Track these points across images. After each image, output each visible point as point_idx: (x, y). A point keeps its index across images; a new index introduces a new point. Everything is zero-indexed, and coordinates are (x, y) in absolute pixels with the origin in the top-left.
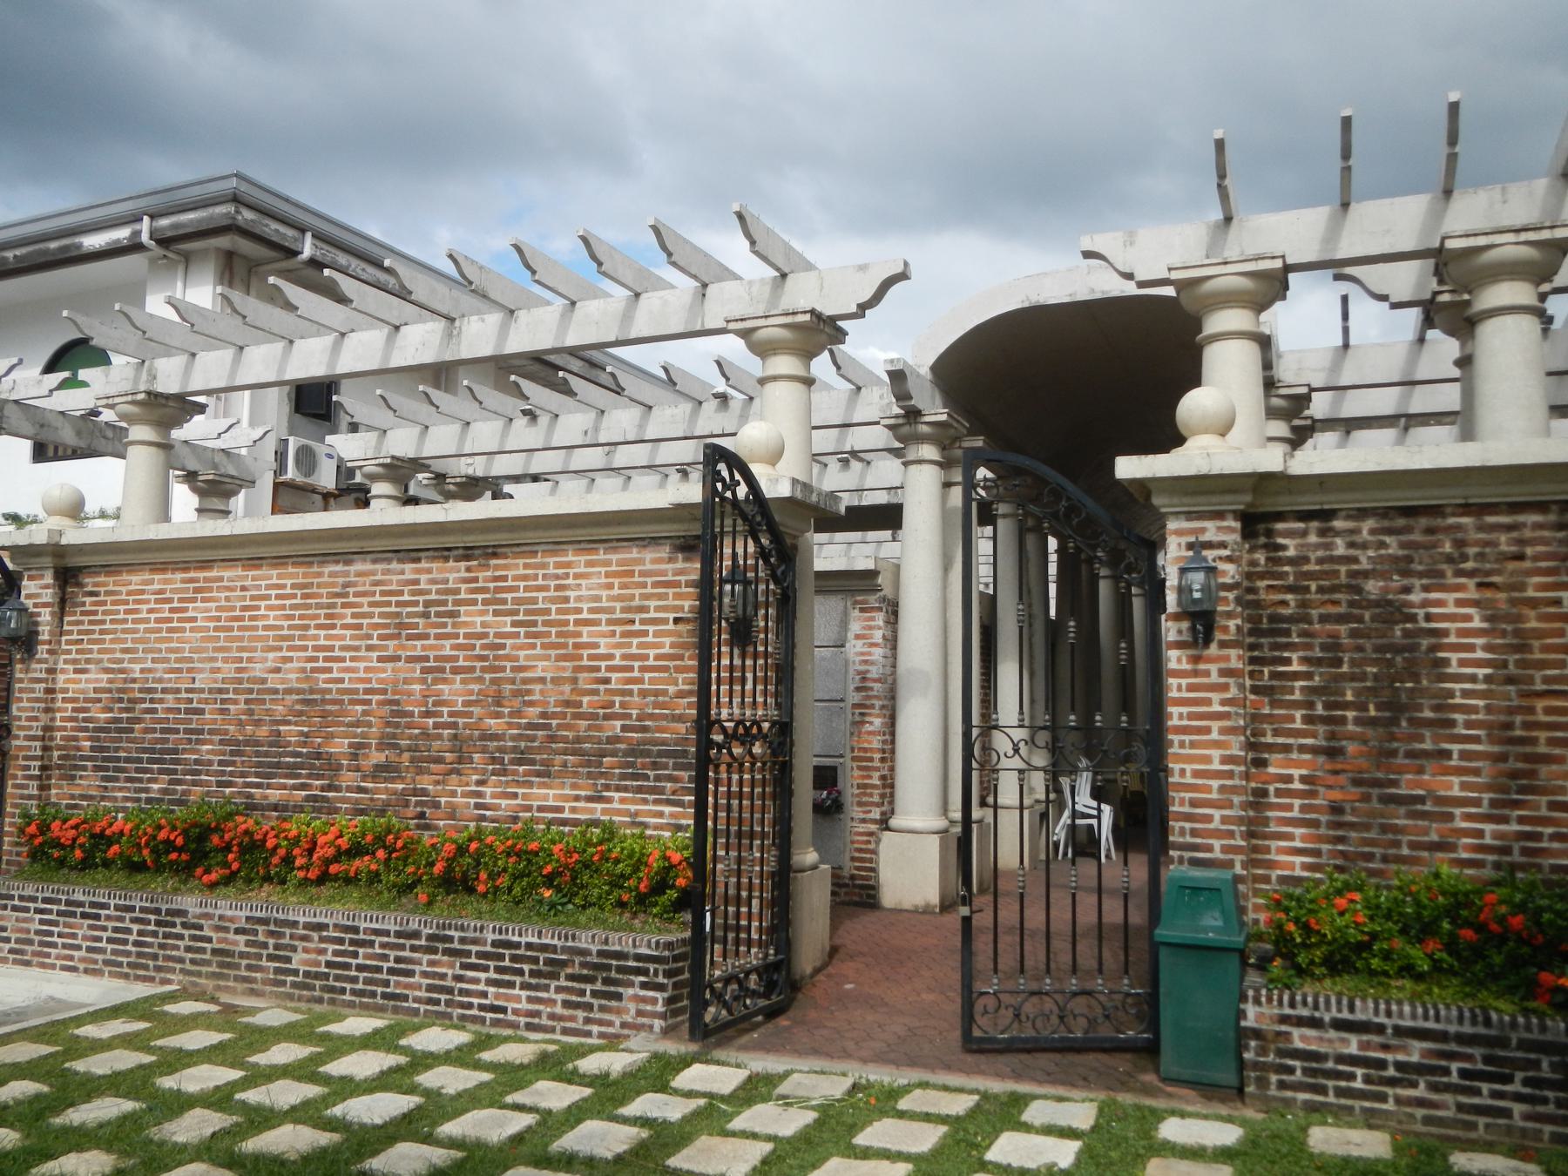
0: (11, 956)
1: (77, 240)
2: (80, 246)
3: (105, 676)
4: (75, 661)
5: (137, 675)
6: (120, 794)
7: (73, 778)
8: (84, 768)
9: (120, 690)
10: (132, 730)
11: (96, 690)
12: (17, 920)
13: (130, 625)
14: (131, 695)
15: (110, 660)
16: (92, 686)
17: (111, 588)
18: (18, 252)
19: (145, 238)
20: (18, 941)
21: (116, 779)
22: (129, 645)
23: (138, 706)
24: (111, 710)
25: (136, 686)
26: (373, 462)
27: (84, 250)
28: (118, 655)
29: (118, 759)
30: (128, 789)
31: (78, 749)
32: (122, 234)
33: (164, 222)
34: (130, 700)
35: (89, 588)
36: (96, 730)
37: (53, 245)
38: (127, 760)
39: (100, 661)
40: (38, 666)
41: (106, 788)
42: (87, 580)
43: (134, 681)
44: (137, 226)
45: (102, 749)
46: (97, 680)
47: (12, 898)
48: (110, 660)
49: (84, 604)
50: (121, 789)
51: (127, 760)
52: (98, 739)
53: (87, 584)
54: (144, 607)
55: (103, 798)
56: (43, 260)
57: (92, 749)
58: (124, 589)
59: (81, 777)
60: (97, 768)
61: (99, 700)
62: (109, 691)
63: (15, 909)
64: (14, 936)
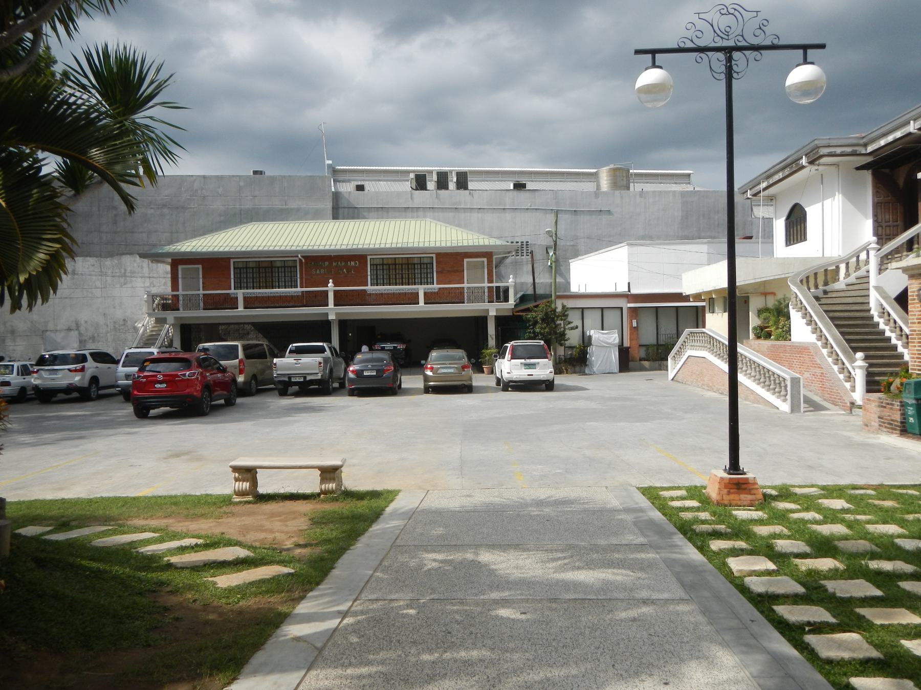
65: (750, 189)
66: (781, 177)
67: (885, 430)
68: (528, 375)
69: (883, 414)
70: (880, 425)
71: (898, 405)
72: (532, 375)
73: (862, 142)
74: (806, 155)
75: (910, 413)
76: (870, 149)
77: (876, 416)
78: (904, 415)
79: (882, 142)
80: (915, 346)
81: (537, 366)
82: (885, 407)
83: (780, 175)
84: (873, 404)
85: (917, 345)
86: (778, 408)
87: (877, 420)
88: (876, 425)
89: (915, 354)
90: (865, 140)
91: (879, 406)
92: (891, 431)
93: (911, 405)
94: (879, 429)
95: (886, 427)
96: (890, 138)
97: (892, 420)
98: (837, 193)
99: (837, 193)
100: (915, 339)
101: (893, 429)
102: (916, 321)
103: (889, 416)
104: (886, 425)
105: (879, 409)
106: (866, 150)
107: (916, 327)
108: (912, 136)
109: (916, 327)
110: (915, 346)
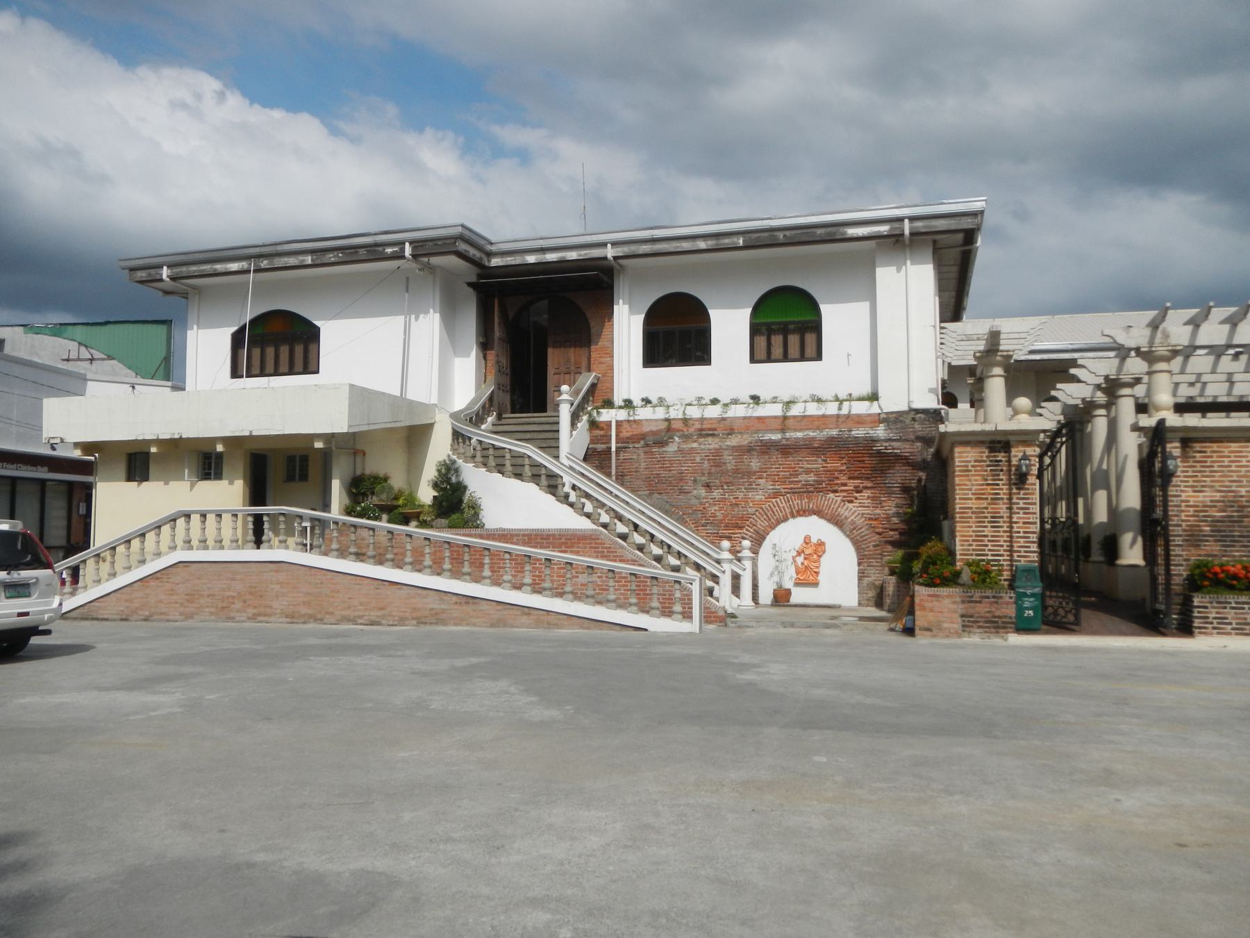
0: (1233, 632)
1: (841, 229)
2: (845, 233)
3: (1218, 494)
4: (1193, 486)
5: (1243, 494)
6: (1237, 554)
7: (1199, 546)
8: (1207, 541)
9: (1229, 501)
10: (1242, 522)
11: (1211, 501)
12: (1236, 613)
13: (1234, 469)
14: (1240, 504)
15: (1221, 486)
16: (1208, 499)
17: (1215, 449)
18: (787, 233)
19: (907, 232)
20: (1237, 624)
21: (1234, 546)
22: (1235, 478)
23: (1246, 509)
24: (1224, 511)
25: (1244, 499)
26: (1131, 376)
27: (847, 236)
28: (1227, 484)
29: (1234, 536)
30: (1244, 551)
31: (1202, 531)
32: (884, 229)
33: (919, 224)
34: (1239, 506)
35: (1198, 449)
36: (1212, 521)
37: (819, 231)
38: (1240, 536)
39: (1213, 487)
40: (1174, 489)
41: (1226, 551)
42: (1195, 445)
43: (1242, 496)
44: (896, 225)
45: (1219, 531)
46: (1211, 496)
47: (1230, 603)
48: (1221, 486)
49: (1195, 457)
50: (1237, 551)
51: (1240, 536)
52: (1216, 526)
53: (1195, 447)
54: (1244, 459)
55: (1224, 556)
56: (811, 239)
57: (1212, 531)
58: (1226, 450)
59: (1205, 546)
60: (1216, 541)
61: (1215, 506)
62: (1223, 502)
63: (1234, 608)
64: (1234, 622)
65: (169, 267)
66: (310, 262)
67: (979, 630)
68: (20, 615)
69: (971, 611)
70: (963, 626)
71: (1011, 598)
72: (26, 614)
73: (489, 248)
74: (411, 243)
75: (1026, 605)
76: (495, 262)
77: (957, 615)
78: (1020, 610)
79: (531, 259)
80: (971, 527)
81: (32, 589)
82: (980, 602)
83: (308, 260)
84: (947, 601)
85: (974, 525)
86: (646, 630)
87: (960, 620)
88: (957, 626)
89: (971, 536)
90: (493, 248)
91: (963, 602)
92: (994, 630)
93: (1033, 595)
94: (964, 631)
95: (980, 627)
96: (551, 257)
97: (995, 617)
98: (431, 310)
99: (431, 310)
100: (971, 518)
101: (995, 628)
102: (970, 496)
103: (989, 612)
104: (981, 624)
105: (961, 606)
106: (489, 261)
107: (972, 503)
108: (605, 263)
109: (972, 503)
110: (971, 527)
